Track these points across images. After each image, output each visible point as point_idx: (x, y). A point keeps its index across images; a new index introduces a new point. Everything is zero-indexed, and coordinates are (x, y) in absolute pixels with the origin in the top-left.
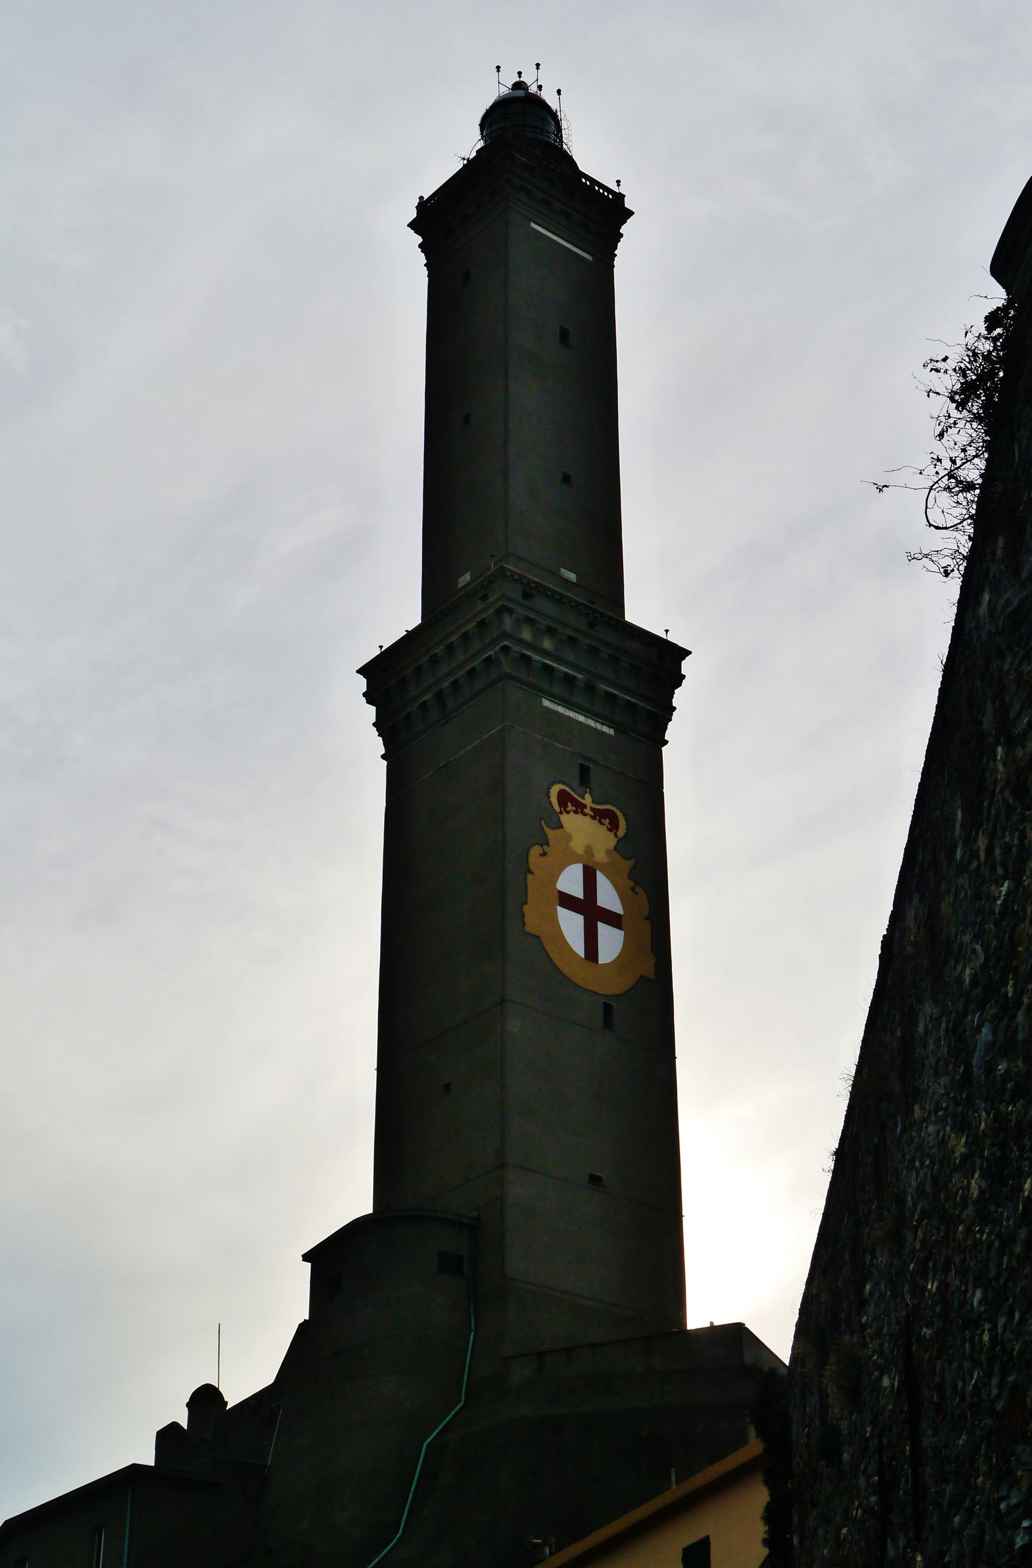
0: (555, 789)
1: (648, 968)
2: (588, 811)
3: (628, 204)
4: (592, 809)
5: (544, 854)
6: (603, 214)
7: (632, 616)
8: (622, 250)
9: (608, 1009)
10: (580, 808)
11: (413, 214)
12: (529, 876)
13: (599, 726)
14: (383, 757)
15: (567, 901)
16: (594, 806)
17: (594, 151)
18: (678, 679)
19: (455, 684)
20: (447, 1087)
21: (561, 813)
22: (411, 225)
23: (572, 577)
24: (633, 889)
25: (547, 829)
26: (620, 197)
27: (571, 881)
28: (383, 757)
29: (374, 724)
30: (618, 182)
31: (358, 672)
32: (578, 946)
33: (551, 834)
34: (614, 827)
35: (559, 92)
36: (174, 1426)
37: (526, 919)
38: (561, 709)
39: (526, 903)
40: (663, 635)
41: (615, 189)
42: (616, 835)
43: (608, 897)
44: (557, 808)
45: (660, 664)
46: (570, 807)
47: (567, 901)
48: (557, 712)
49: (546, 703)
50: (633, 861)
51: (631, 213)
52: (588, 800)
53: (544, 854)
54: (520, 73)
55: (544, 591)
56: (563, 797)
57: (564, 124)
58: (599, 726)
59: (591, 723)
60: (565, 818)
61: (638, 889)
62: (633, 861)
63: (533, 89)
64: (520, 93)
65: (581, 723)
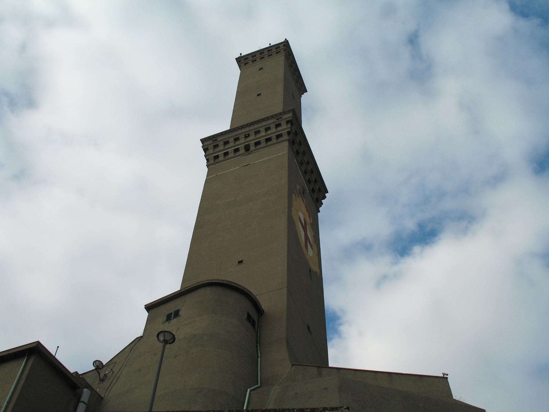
9: (310, 271)
10: (303, 200)
18: (324, 197)
34: (310, 217)
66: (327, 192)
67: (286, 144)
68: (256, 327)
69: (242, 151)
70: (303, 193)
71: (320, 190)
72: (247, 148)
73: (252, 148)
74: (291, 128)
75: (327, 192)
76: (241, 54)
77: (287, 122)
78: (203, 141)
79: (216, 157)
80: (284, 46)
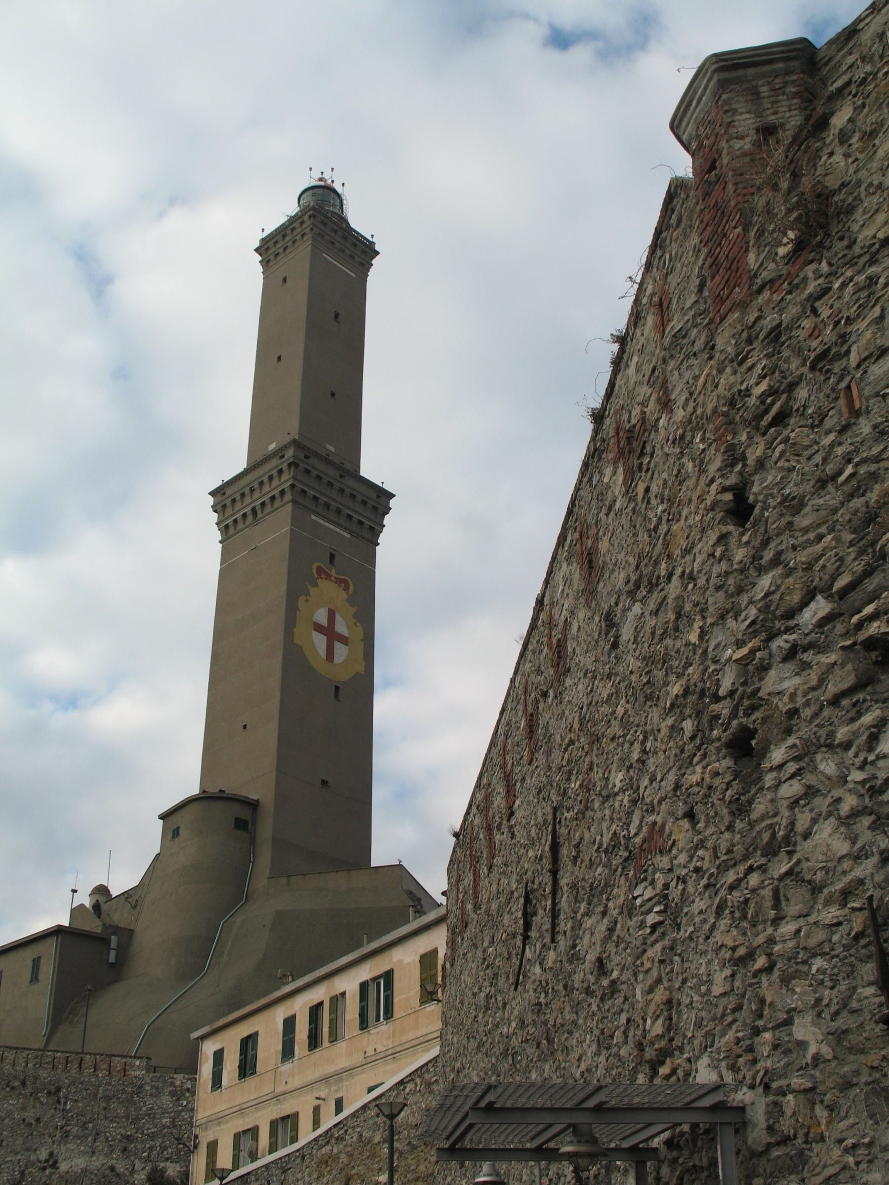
0: (315, 565)
2: (332, 578)
3: (377, 248)
5: (307, 601)
6: (363, 252)
7: (365, 472)
8: (372, 273)
9: (337, 689)
10: (328, 577)
11: (257, 244)
14: (221, 542)
15: (318, 628)
17: (360, 218)
18: (387, 510)
19: (263, 504)
20: (245, 726)
22: (257, 250)
23: (332, 449)
25: (309, 587)
26: (373, 243)
28: (221, 542)
29: (217, 524)
30: (372, 236)
31: (210, 494)
32: (322, 651)
33: (312, 590)
34: (347, 588)
35: (343, 184)
36: (82, 906)
38: (322, 522)
40: (381, 485)
41: (371, 239)
43: (341, 627)
44: (316, 575)
45: (378, 500)
46: (323, 576)
47: (318, 628)
49: (313, 517)
51: (377, 253)
52: (333, 572)
53: (307, 601)
54: (322, 173)
55: (316, 454)
56: (320, 570)
57: (345, 202)
60: (319, 582)
61: (358, 624)
63: (329, 182)
64: (322, 183)
66: (392, 496)
67: (290, 506)
68: (250, 826)
69: (250, 518)
71: (375, 509)
72: (254, 510)
73: (260, 515)
74: (294, 478)
75: (392, 496)
76: (263, 230)
77: (290, 465)
78: (212, 494)
79: (227, 526)
80: (310, 216)
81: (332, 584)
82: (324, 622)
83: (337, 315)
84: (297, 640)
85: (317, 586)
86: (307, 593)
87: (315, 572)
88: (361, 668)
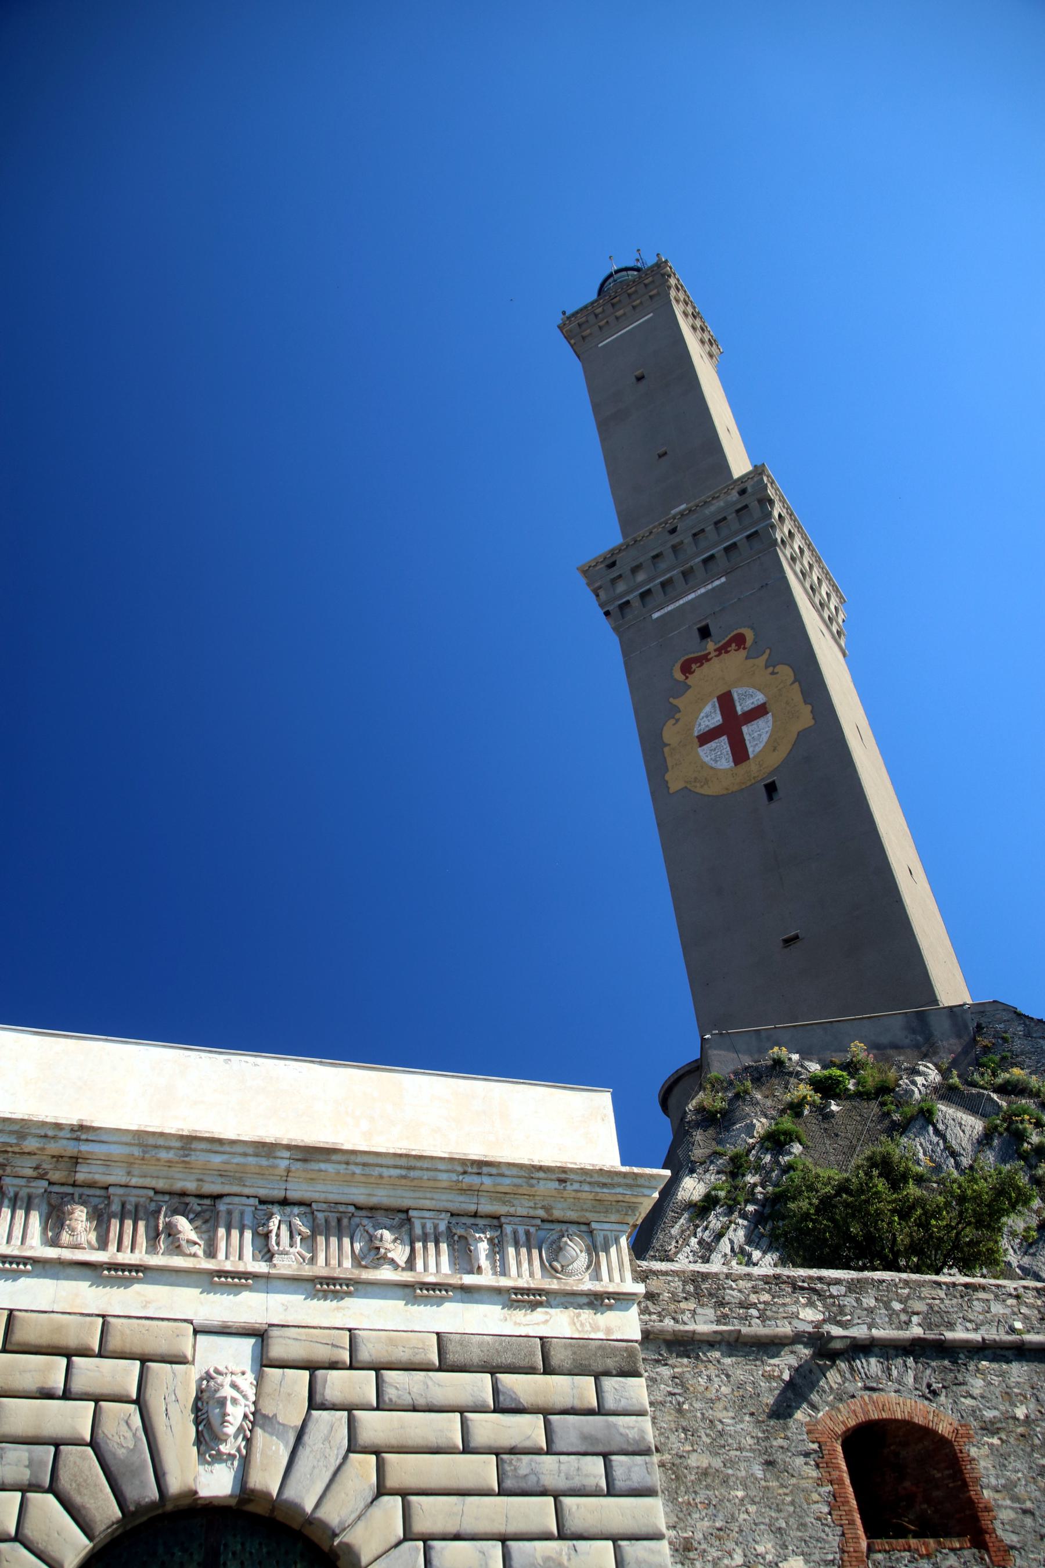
1: (805, 719)
4: (715, 650)
5: (677, 720)
9: (771, 789)
12: (666, 750)
13: (710, 587)
15: (705, 738)
16: (717, 646)
21: (687, 678)
24: (773, 673)
27: (711, 717)
37: (670, 785)
39: (667, 770)
42: (744, 648)
46: (694, 666)
47: (705, 738)
48: (669, 613)
49: (655, 616)
50: (768, 651)
58: (710, 587)
59: (703, 590)
60: (689, 682)
61: (778, 669)
62: (768, 651)
65: (692, 599)
70: (705, 633)
81: (715, 660)
82: (717, 719)
83: (640, 379)
84: (675, 786)
85: (689, 687)
86: (674, 711)
87: (679, 676)
88: (805, 719)
